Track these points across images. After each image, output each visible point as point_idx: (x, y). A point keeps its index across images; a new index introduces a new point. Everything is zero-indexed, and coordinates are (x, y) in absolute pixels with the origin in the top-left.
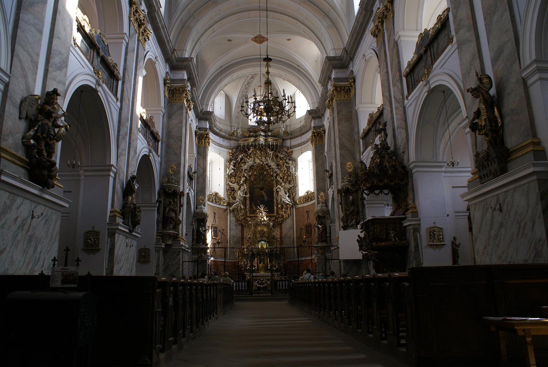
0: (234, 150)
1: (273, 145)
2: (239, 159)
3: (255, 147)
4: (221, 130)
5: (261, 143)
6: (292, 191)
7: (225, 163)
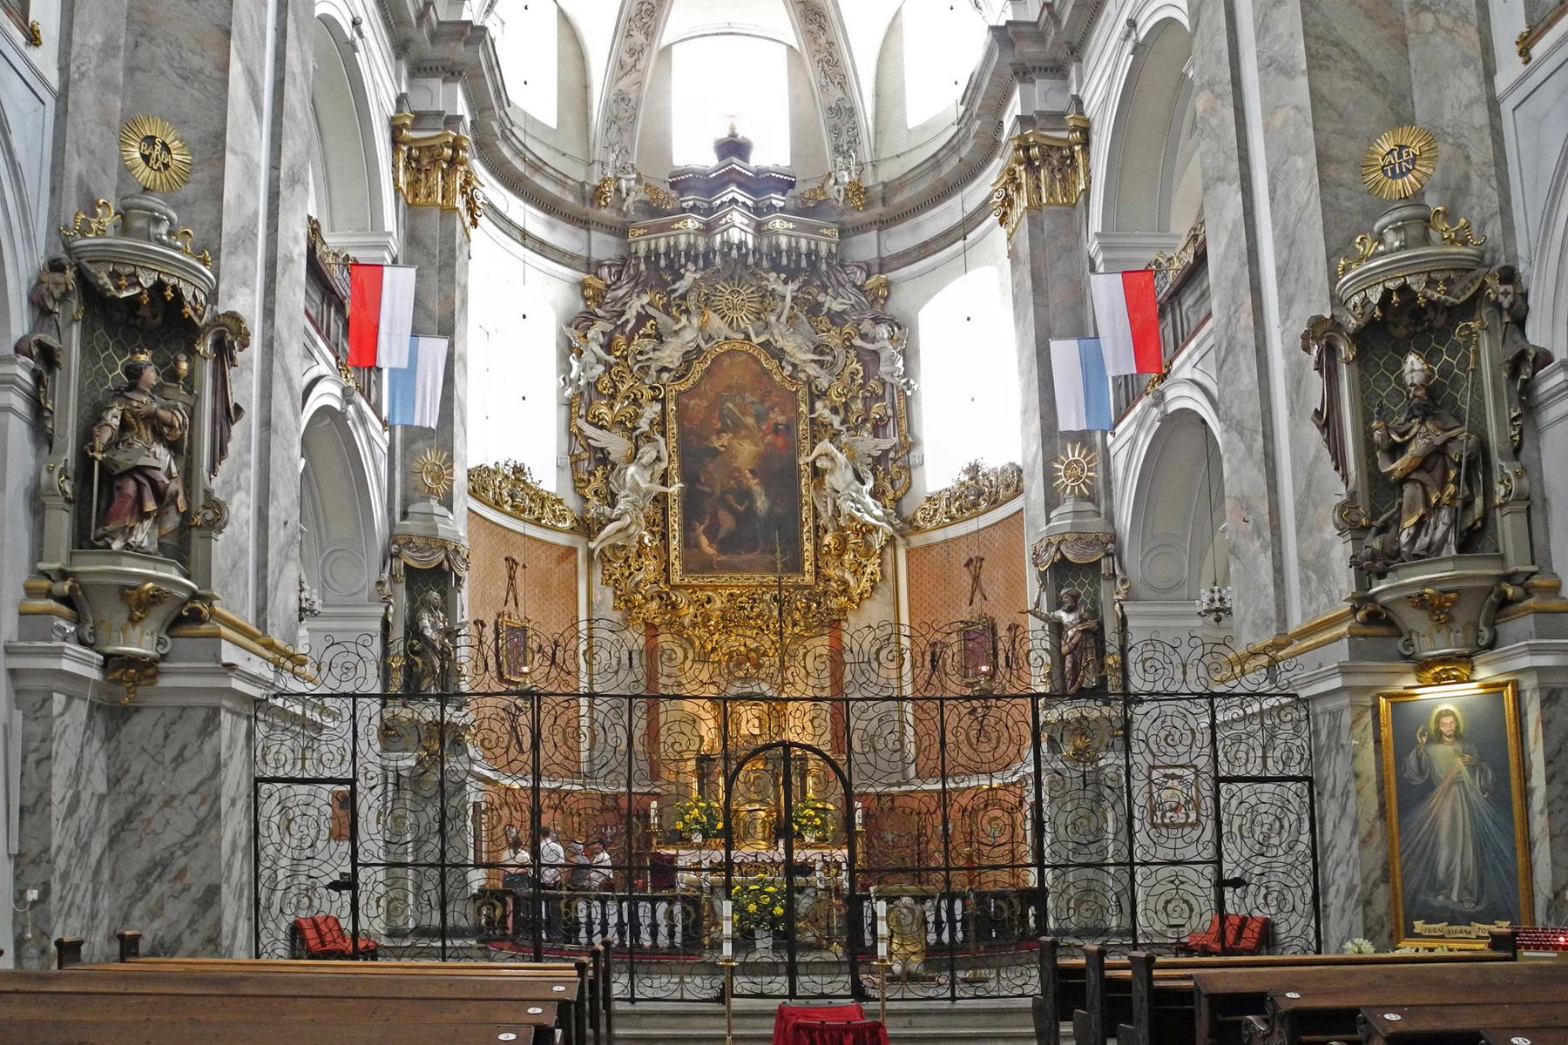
0: (605, 272)
1: (793, 251)
2: (631, 314)
3: (708, 263)
4: (538, 166)
5: (735, 236)
6: (891, 469)
7: (561, 332)
